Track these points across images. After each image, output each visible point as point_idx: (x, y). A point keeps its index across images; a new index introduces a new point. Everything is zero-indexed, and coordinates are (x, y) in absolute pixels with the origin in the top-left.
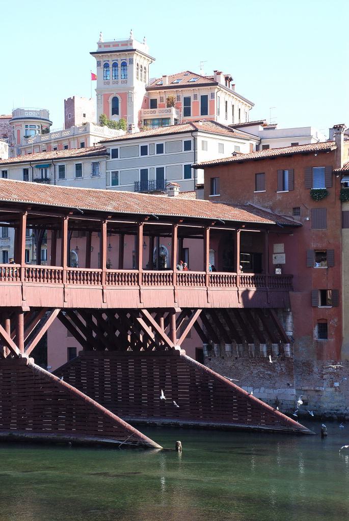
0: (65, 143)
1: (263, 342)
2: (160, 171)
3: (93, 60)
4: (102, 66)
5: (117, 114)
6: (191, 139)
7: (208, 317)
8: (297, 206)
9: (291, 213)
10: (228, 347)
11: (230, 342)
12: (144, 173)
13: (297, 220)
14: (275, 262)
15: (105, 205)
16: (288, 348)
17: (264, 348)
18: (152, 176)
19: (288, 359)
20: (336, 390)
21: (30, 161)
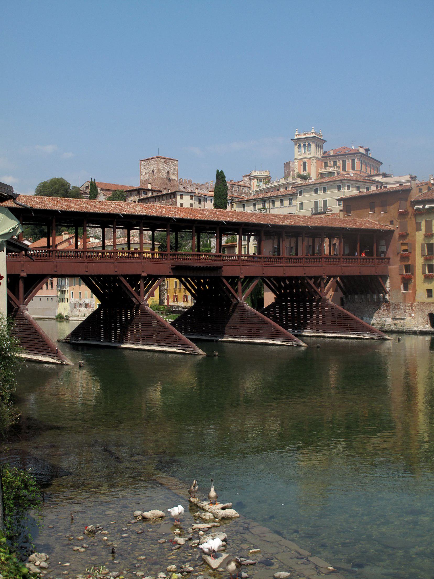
0: (277, 188)
1: (374, 293)
2: (325, 202)
6: (341, 184)
7: (345, 281)
8: (392, 220)
9: (389, 224)
10: (356, 297)
11: (357, 294)
12: (316, 203)
13: (391, 227)
14: (381, 250)
15: (284, 222)
16: (387, 297)
17: (375, 297)
18: (321, 205)
20: (412, 318)
21: (257, 199)
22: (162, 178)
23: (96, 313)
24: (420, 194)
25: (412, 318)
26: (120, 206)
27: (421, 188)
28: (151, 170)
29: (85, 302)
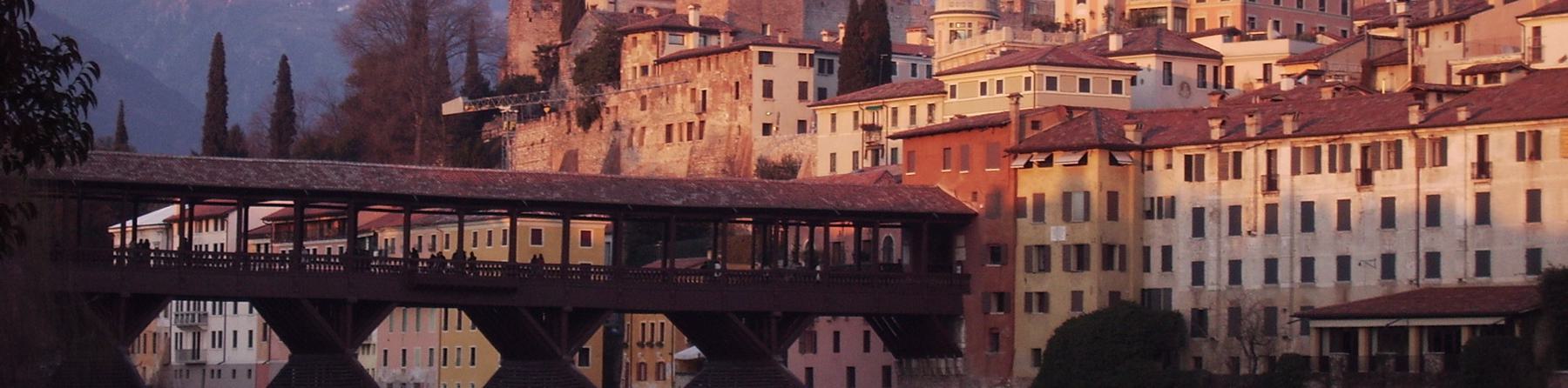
1: (942, 357)
9: (970, 198)
10: (914, 363)
15: (678, 198)
17: (942, 363)
19: (962, 375)
23: (285, 371)
24: (1036, 132)
26: (318, 171)
27: (1037, 119)
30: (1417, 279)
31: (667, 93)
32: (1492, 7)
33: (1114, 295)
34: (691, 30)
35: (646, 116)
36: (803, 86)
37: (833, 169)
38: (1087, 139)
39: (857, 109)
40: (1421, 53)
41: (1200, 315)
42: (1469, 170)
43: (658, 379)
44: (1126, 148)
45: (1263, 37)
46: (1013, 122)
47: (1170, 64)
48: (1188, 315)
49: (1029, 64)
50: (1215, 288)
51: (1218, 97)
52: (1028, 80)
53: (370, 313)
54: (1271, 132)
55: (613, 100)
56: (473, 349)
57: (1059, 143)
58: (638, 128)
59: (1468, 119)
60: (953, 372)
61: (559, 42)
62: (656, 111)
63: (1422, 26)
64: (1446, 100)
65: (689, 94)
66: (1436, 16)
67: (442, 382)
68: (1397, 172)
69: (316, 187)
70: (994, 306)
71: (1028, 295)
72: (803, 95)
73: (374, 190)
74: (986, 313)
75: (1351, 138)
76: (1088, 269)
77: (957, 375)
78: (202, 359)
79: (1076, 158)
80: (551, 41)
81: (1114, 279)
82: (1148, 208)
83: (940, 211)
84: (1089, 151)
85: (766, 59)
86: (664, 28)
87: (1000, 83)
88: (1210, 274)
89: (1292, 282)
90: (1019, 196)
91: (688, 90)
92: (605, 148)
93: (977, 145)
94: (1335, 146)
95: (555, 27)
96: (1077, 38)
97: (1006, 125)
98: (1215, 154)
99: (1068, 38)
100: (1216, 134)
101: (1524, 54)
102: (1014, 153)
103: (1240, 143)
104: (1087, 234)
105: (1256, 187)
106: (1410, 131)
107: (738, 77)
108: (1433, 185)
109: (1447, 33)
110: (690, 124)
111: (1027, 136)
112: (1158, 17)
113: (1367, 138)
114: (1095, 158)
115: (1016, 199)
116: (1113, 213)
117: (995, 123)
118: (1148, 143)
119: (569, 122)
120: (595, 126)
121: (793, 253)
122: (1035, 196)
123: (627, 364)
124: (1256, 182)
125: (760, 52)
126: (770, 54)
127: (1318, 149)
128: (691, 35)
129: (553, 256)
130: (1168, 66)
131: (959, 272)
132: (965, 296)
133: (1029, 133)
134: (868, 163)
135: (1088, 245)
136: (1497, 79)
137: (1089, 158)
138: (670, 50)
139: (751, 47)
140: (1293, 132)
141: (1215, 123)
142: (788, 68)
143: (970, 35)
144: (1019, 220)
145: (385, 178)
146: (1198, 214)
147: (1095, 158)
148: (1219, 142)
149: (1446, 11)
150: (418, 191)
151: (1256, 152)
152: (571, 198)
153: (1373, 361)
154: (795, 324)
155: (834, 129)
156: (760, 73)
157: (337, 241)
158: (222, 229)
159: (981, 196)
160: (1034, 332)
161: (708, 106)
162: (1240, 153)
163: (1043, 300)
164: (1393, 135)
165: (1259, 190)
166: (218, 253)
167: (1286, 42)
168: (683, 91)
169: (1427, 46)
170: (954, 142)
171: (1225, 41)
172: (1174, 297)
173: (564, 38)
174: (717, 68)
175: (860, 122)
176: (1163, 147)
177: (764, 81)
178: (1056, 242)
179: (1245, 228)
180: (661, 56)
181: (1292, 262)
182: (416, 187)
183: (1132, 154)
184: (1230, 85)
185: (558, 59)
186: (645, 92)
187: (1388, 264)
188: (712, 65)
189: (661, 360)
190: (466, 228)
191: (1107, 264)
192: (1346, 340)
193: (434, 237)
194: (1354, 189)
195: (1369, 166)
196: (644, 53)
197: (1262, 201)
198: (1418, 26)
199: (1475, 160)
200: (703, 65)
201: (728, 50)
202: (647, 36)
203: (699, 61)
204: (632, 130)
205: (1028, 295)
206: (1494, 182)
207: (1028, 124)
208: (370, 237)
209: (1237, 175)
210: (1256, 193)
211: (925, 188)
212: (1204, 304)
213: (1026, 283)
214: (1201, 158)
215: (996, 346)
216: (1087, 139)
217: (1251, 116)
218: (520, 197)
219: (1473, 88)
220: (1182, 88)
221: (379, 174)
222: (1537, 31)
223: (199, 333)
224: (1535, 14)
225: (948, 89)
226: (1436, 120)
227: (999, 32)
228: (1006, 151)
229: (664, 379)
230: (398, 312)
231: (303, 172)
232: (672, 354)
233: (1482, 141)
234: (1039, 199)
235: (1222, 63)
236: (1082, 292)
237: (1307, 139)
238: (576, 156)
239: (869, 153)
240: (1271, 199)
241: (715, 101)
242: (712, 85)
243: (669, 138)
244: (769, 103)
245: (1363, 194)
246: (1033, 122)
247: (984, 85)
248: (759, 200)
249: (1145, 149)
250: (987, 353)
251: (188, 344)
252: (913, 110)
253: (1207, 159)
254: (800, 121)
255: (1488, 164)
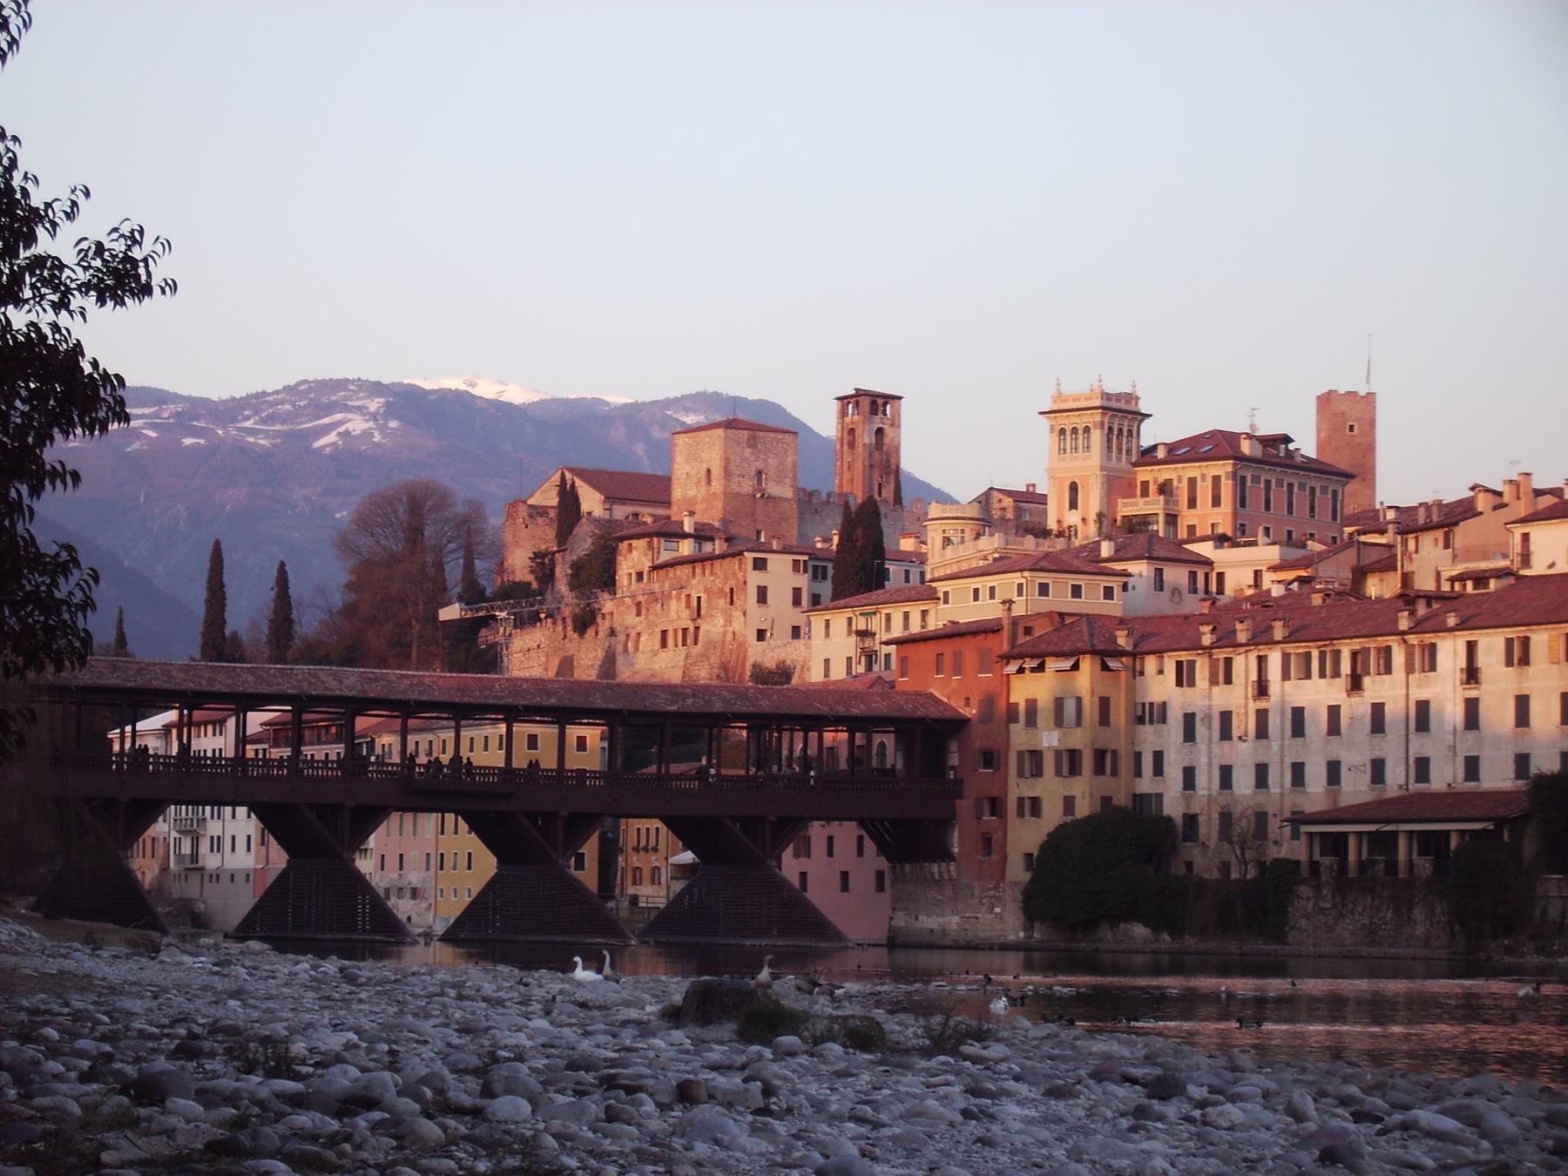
1: (935, 862)
3: (1044, 423)
4: (1057, 433)
5: (1076, 508)
9: (963, 704)
10: (907, 867)
11: (909, 863)
15: (673, 703)
17: (935, 868)
20: (997, 918)
22: (738, 494)
23: (283, 877)
24: (1028, 638)
25: (997, 918)
26: (316, 676)
27: (1029, 625)
28: (704, 467)
29: (410, 883)
30: (1407, 784)
31: (662, 598)
32: (1481, 513)
33: (1106, 801)
34: (686, 536)
35: (641, 622)
36: (797, 593)
37: (827, 674)
38: (1079, 644)
39: (851, 615)
40: (1411, 559)
41: (1191, 820)
42: (1458, 676)
43: (653, 883)
44: (1118, 653)
45: (1253, 544)
46: (1006, 628)
47: (1161, 570)
48: (1179, 820)
49: (1021, 571)
50: (1206, 793)
51: (1209, 603)
52: (1020, 585)
53: (368, 818)
54: (1261, 638)
55: (608, 606)
56: (470, 854)
57: (1051, 649)
58: (633, 634)
59: (1457, 625)
60: (946, 876)
61: (555, 549)
62: (651, 617)
63: (1412, 532)
64: (1435, 606)
65: (684, 600)
66: (1426, 523)
67: (439, 887)
68: (1386, 677)
69: (314, 693)
70: (987, 811)
71: (1021, 800)
72: (797, 601)
73: (372, 695)
74: (979, 818)
75: (1341, 644)
76: (1080, 774)
77: (951, 880)
78: (200, 864)
79: (1068, 664)
80: (547, 548)
81: (1106, 784)
82: (1139, 713)
83: (933, 716)
84: (1081, 656)
85: (760, 565)
86: (659, 534)
87: (992, 589)
88: (1201, 779)
89: (1282, 787)
90: (1011, 701)
91: (683, 596)
92: (600, 654)
93: (970, 650)
94: (1325, 652)
95: (551, 533)
96: (1069, 545)
97: (998, 630)
98: (1207, 660)
99: (1060, 544)
100: (1207, 640)
101: (1512, 561)
102: (1007, 658)
103: (1231, 649)
104: (1079, 739)
105: (1246, 693)
106: (1399, 637)
107: (732, 583)
108: (1423, 691)
109: (1436, 539)
110: (685, 630)
111: (1019, 642)
112: (1149, 523)
113: (1357, 644)
114: (1086, 664)
115: (1009, 704)
116: (1104, 718)
117: (988, 629)
118: (1139, 649)
119: (565, 628)
120: (591, 632)
121: (787, 758)
122: (1028, 701)
123: (623, 868)
124: (1246, 688)
125: (755, 558)
126: (765, 560)
127: (1308, 655)
128: (686, 541)
129: (548, 761)
130: (1159, 572)
131: (952, 777)
132: (958, 801)
133: (1022, 639)
134: (861, 669)
135: (1080, 750)
136: (1486, 585)
137: (1081, 664)
138: (665, 556)
139: (745, 554)
140: (1284, 638)
141: (1206, 629)
142: (782, 574)
143: (963, 541)
144: (1011, 725)
145: (382, 683)
146: (1189, 719)
147: (1086, 664)
148: (1210, 648)
149: (1435, 518)
150: (415, 696)
151: (1246, 658)
152: (566, 703)
153: (1363, 866)
154: (789, 829)
155: (827, 635)
156: (755, 579)
157: (334, 746)
158: (221, 734)
159: (974, 702)
160: (1026, 837)
161: (703, 612)
162: (1231, 659)
163: (1035, 805)
164: (1382, 641)
165: (1250, 696)
166: (217, 758)
167: (1277, 548)
168: (678, 597)
169: (1416, 552)
170: (947, 648)
171: (1216, 547)
172: (1165, 801)
173: (559, 544)
174: (712, 574)
175: (854, 628)
176: (1154, 653)
177: (758, 587)
178: (1049, 747)
179: (1236, 733)
180: (656, 563)
181: (1282, 767)
182: (413, 692)
183: (1124, 659)
184: (1221, 591)
185: (554, 565)
186: (640, 598)
187: (1378, 769)
188: (707, 572)
189: (657, 864)
190: (462, 733)
191: (1099, 769)
192: (1336, 844)
193: (431, 742)
194: (1344, 695)
195: (1359, 672)
196: (639, 559)
197: (1253, 706)
198: (1407, 533)
199: (1464, 665)
200: (698, 571)
201: (722, 557)
202: (641, 544)
203: (694, 568)
204: (628, 636)
205: (1021, 800)
206: (1484, 687)
207: (1021, 630)
208: (367, 743)
209: (1228, 680)
210: (1246, 698)
211: (918, 694)
212: (1195, 809)
213: (1018, 788)
214: (1192, 664)
215: (988, 850)
216: (1079, 644)
217: (1241, 622)
218: (516, 702)
219: (1462, 595)
220: (1173, 595)
221: (376, 680)
222: (1526, 537)
223: (197, 838)
224: (1523, 521)
225: (941, 595)
226: (1425, 626)
227: (992, 539)
228: (998, 657)
229: (660, 883)
230: (395, 818)
231: (300, 677)
232: (667, 859)
233: (1471, 647)
234: (1032, 705)
235: (1213, 569)
236: (1074, 797)
237: (1297, 644)
238: (572, 661)
239: (863, 658)
240: (1262, 704)
241: (709, 607)
242: (706, 591)
243: (664, 644)
244: (763, 610)
245: (1353, 699)
246: (1025, 628)
247: (976, 591)
248: (753, 706)
249: (1136, 655)
250: (980, 857)
251: (186, 849)
252: (906, 616)
253: (1198, 664)
254: (794, 627)
255: (1477, 669)
